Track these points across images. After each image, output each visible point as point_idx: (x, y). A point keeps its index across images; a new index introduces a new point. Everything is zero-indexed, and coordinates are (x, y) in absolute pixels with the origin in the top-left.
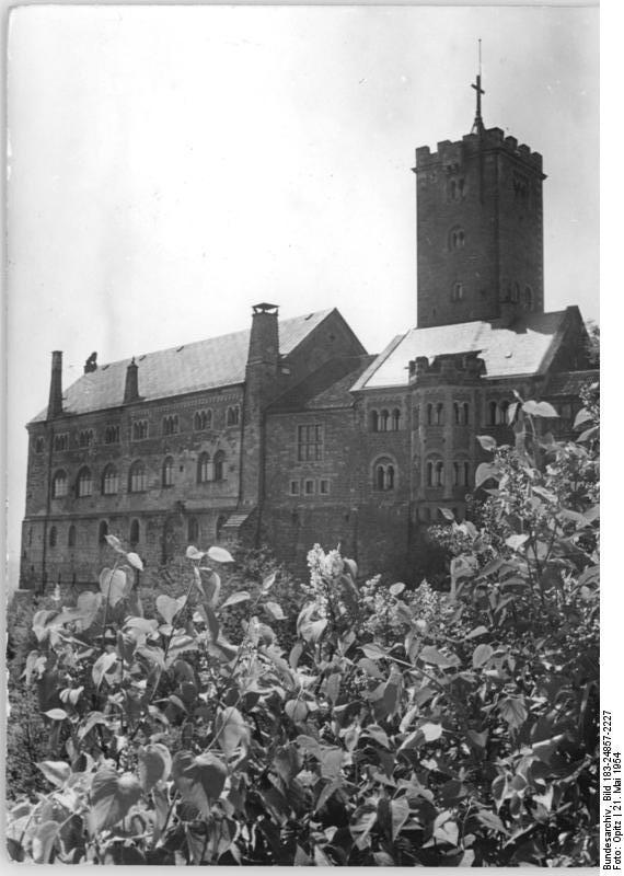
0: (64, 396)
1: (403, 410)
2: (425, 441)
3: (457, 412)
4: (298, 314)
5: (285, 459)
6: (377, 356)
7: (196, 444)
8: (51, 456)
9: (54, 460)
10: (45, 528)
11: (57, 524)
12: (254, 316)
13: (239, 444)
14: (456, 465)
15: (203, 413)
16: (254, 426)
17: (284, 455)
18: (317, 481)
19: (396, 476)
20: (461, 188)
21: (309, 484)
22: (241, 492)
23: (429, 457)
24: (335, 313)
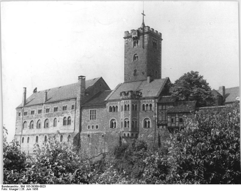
0: (27, 100)
1: (119, 106)
2: (124, 115)
3: (133, 107)
4: (91, 77)
5: (86, 119)
6: (112, 91)
7: (63, 115)
8: (23, 117)
9: (23, 118)
10: (21, 138)
11: (24, 137)
12: (79, 79)
13: (74, 115)
14: (133, 122)
15: (65, 106)
16: (78, 110)
17: (86, 118)
18: (95, 126)
19: (117, 124)
20: (137, 43)
21: (93, 126)
22: (75, 128)
23: (125, 119)
24: (101, 78)
